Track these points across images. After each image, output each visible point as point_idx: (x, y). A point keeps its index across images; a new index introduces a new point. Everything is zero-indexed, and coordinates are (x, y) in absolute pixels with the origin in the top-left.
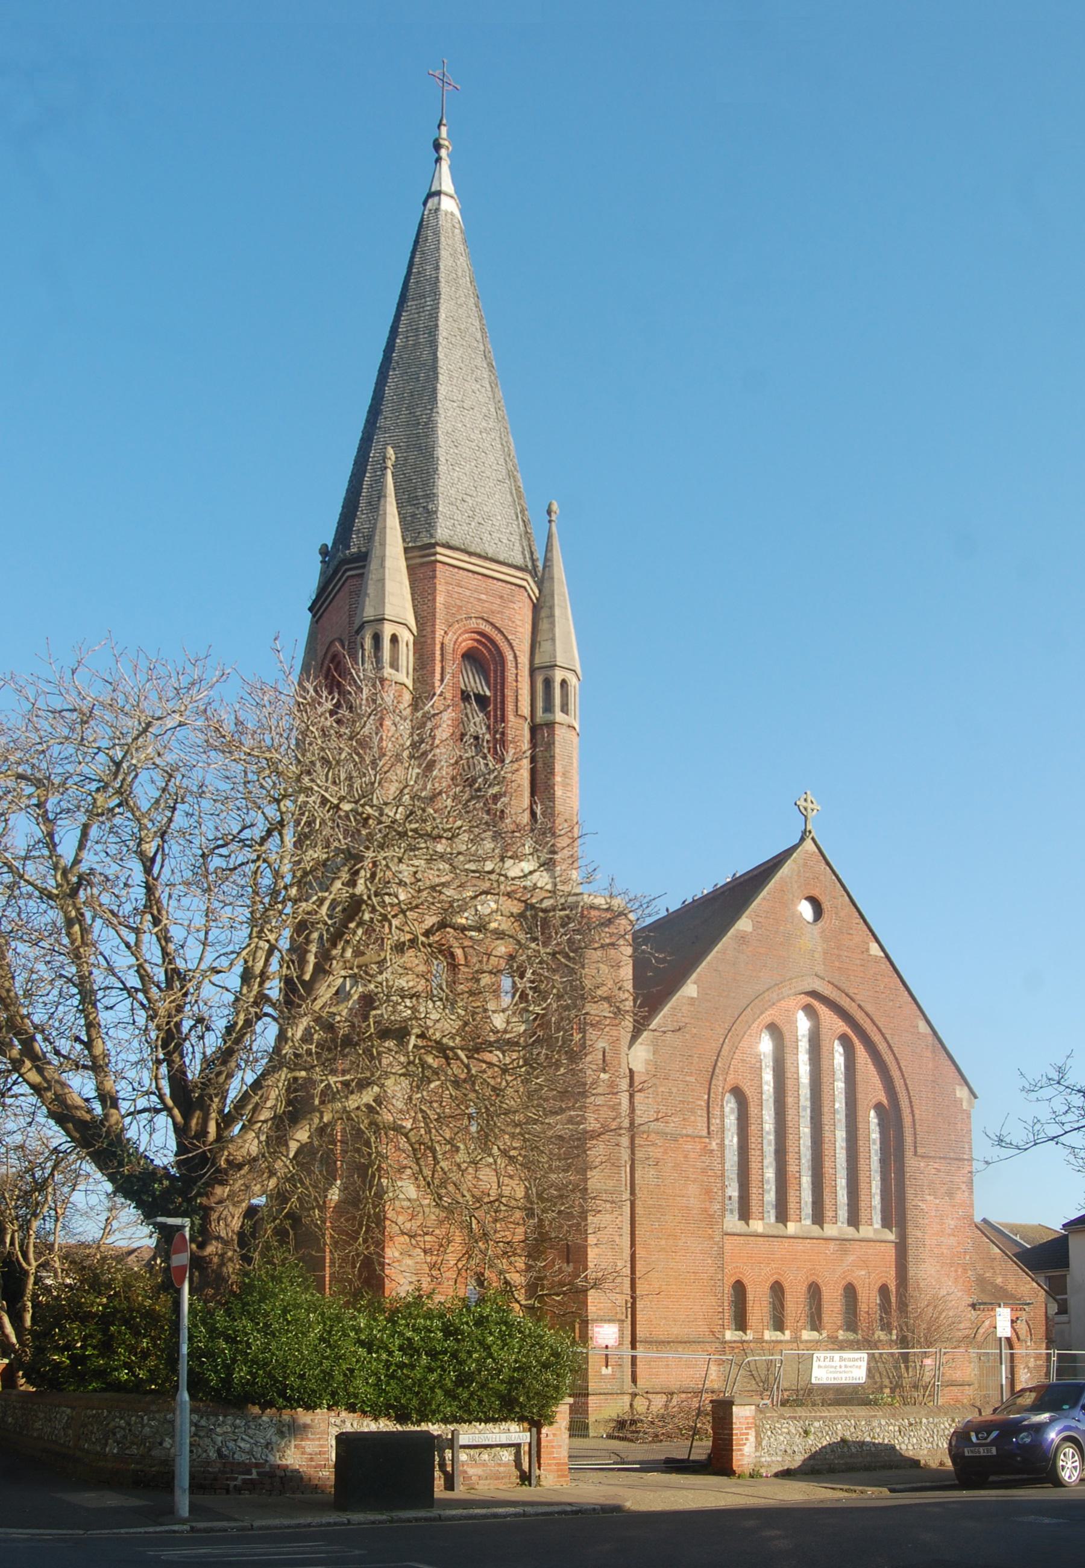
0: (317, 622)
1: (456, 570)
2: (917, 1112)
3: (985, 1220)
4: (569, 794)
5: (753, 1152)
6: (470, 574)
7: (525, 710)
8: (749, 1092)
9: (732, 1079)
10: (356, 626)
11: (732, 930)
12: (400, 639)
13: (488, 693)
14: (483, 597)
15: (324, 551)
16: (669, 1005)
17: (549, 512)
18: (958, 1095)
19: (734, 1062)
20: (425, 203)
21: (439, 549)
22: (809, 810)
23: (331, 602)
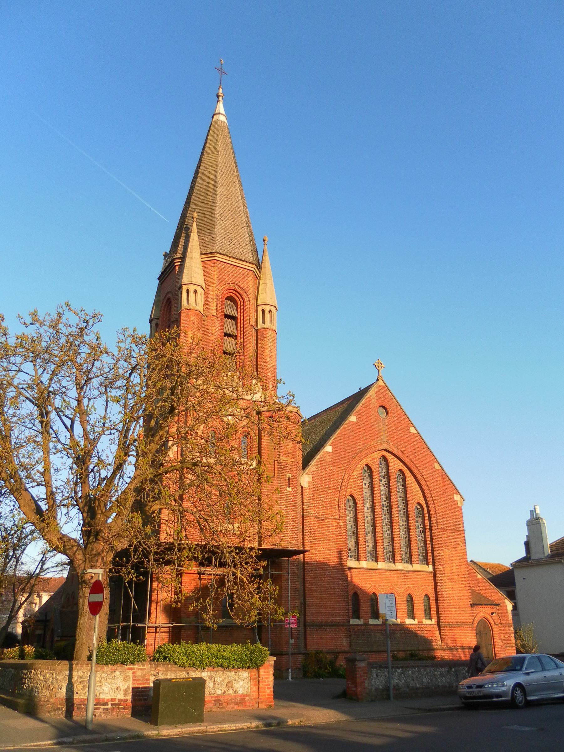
0: (161, 284)
1: (223, 263)
2: (437, 507)
3: (472, 561)
4: (272, 360)
5: (360, 527)
6: (230, 265)
7: (253, 323)
8: (358, 498)
9: (349, 491)
10: (179, 286)
11: (347, 422)
12: (198, 292)
13: (237, 316)
14: (235, 275)
15: (166, 255)
16: (319, 455)
17: (264, 241)
18: (456, 498)
19: (350, 483)
20: (213, 117)
21: (216, 255)
22: (380, 367)
23: (169, 274)
